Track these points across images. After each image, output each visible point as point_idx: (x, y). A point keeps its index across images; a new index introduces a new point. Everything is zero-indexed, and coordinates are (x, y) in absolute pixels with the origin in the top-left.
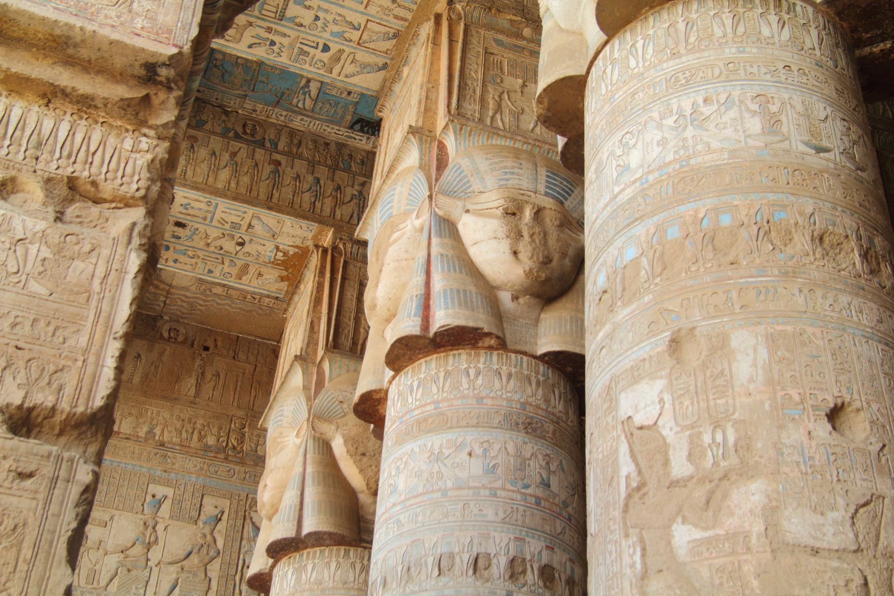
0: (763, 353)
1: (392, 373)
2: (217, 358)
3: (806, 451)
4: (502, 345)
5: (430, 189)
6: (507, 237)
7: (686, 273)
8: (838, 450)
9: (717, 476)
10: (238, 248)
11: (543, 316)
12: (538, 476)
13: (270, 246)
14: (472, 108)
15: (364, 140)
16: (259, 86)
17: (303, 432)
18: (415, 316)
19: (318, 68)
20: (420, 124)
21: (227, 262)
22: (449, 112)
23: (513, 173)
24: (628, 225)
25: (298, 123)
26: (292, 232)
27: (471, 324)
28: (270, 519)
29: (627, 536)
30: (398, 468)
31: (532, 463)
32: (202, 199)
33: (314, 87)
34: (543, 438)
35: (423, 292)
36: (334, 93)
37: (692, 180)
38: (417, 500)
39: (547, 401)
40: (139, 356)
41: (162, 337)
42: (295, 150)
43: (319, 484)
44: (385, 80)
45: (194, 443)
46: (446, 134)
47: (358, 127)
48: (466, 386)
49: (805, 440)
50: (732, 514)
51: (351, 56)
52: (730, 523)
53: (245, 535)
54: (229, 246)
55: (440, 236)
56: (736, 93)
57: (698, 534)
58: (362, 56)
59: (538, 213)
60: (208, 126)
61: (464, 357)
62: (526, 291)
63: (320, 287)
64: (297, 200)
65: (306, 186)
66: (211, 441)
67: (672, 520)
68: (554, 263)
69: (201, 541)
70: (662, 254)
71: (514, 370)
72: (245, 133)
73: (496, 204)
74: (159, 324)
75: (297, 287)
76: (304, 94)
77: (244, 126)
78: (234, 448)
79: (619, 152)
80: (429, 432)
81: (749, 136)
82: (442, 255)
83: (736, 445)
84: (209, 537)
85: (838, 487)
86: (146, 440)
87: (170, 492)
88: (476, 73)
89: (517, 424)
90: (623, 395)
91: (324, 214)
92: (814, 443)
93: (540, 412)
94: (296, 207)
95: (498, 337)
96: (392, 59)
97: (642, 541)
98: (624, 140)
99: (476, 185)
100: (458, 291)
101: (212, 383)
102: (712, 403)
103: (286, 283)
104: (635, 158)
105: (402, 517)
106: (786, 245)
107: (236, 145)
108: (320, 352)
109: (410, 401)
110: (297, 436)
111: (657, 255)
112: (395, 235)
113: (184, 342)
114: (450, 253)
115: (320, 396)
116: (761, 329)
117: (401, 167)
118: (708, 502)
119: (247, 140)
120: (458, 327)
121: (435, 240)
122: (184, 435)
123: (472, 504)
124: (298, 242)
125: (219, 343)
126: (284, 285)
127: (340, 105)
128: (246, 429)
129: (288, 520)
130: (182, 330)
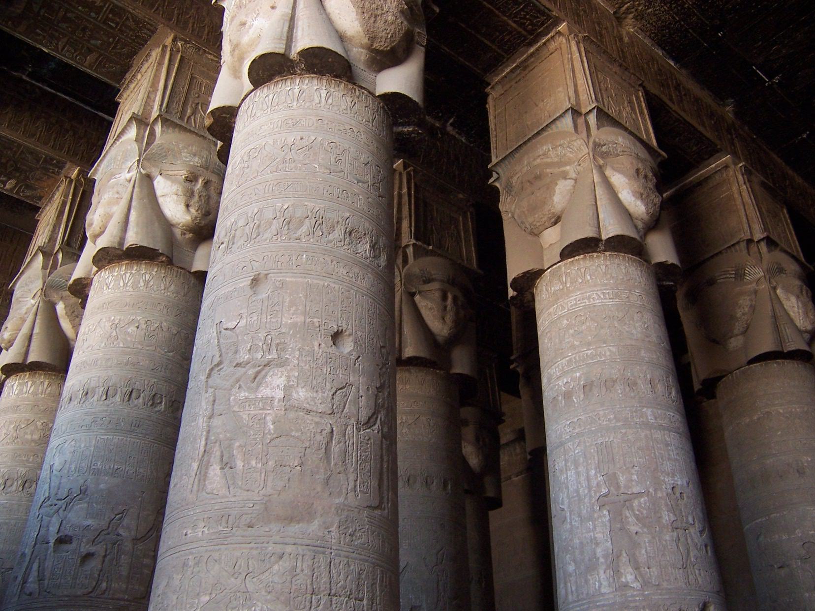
3: (315, 355)
4: (170, 262)
5: (140, 156)
22: (160, 109)
27: (151, 246)
29: (206, 392)
52: (265, 392)
59: (207, 184)
63: (64, 204)
70: (259, 226)
95: (167, 257)
106: (329, 234)
115: (52, 275)
118: (255, 378)
121: (136, 190)
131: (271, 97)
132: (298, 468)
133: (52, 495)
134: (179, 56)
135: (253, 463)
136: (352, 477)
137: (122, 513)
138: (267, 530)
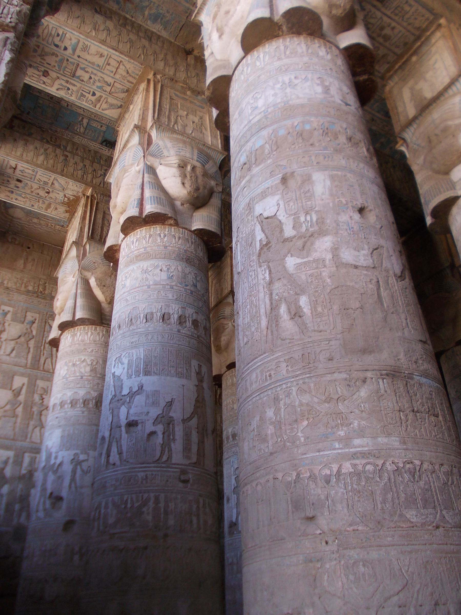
0: (328, 183)
1: (124, 236)
3: (350, 225)
4: (176, 224)
5: (144, 153)
6: (180, 176)
7: (289, 149)
8: (363, 225)
9: (308, 235)
10: (46, 194)
11: (194, 214)
13: (62, 194)
14: (164, 120)
15: (107, 150)
17: (76, 275)
19: (89, 104)
20: (140, 124)
21: (41, 202)
23: (183, 150)
24: (258, 131)
25: (76, 139)
26: (72, 188)
27: (163, 212)
28: (60, 314)
29: (260, 266)
30: (126, 277)
35: (140, 197)
36: (94, 126)
37: (291, 110)
38: (135, 290)
39: (196, 251)
42: (75, 152)
43: (83, 297)
44: (121, 114)
46: (152, 130)
47: (104, 144)
48: (159, 241)
49: (349, 220)
50: (316, 251)
52: (315, 255)
53: (46, 330)
54: (42, 193)
55: (149, 173)
56: (310, 76)
57: (299, 261)
58: (111, 100)
59: (194, 168)
61: (158, 228)
62: (188, 202)
63: (85, 212)
64: (75, 173)
65: (79, 168)
67: (286, 256)
68: (201, 190)
70: (276, 142)
71: (181, 236)
75: (74, 214)
76: (81, 125)
77: (51, 138)
78: (41, 292)
79: (252, 102)
80: (141, 260)
81: (316, 93)
82: (149, 182)
83: (317, 221)
85: (365, 241)
88: (166, 106)
90: (257, 205)
91: (88, 181)
92: (353, 222)
93: (193, 255)
94: (75, 176)
95: (175, 220)
96: (125, 103)
97: (269, 267)
98: (254, 96)
99: (166, 153)
100: (157, 197)
102: (304, 204)
103: (68, 214)
104: (260, 103)
105: (128, 298)
107: (47, 146)
108: (85, 240)
109: (132, 247)
111: (274, 142)
112: (127, 174)
114: (153, 181)
115: (85, 260)
116: (327, 172)
117: (129, 145)
119: (52, 144)
120: (156, 213)
121: (146, 175)
123: (162, 292)
124: (75, 193)
126: (67, 215)
128: (47, 284)
129: (69, 313)
131: (261, 56)
132: (359, 310)
133: (117, 393)
134: (160, 85)
135: (319, 309)
136: (403, 316)
137: (171, 401)
138: (347, 360)
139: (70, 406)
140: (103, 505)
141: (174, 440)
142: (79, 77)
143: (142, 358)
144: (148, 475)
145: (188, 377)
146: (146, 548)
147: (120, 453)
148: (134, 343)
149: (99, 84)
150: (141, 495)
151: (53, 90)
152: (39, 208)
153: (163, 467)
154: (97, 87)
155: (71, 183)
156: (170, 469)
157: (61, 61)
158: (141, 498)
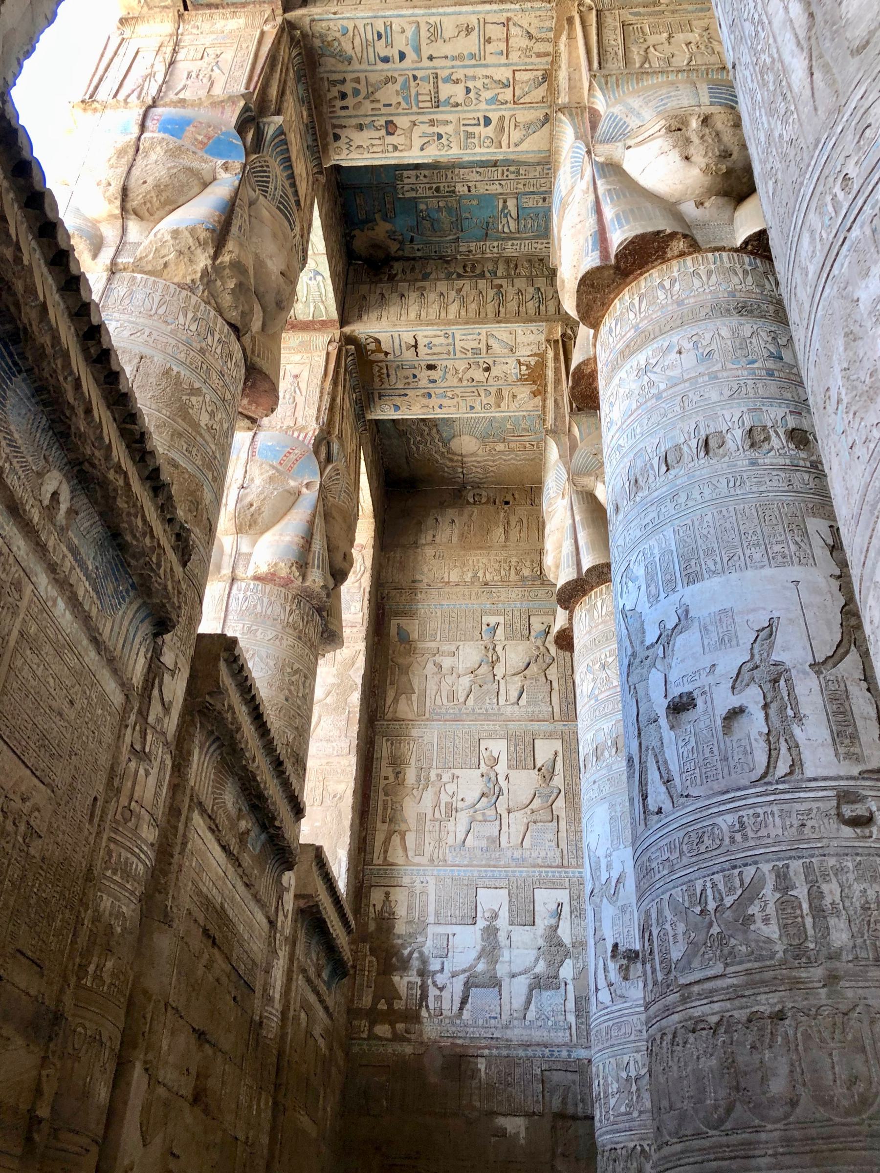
1: (592, 331)
2: (517, 508)
4: (694, 247)
6: (674, 147)
10: (486, 374)
11: (736, 214)
12: (764, 351)
16: (466, 223)
18: (593, 251)
21: (482, 393)
25: (511, 249)
31: (754, 340)
32: (439, 333)
33: (511, 204)
34: (764, 317)
36: (531, 205)
38: (632, 418)
40: (453, 521)
41: (468, 503)
43: (588, 527)
45: (513, 577)
46: (594, 96)
51: (513, 120)
54: (479, 375)
55: (605, 177)
58: (525, 116)
59: (706, 120)
60: (432, 277)
62: (711, 192)
64: (523, 309)
65: (528, 297)
66: (526, 572)
69: (536, 653)
71: (713, 267)
72: (466, 271)
73: (657, 127)
74: (464, 493)
76: (506, 216)
77: (464, 267)
84: (542, 648)
86: (472, 583)
87: (501, 619)
89: (728, 310)
91: (549, 313)
93: (754, 296)
95: (685, 236)
101: (518, 528)
105: (621, 442)
107: (460, 283)
110: (563, 497)
113: (487, 503)
120: (636, 237)
121: (599, 183)
122: (503, 573)
123: (691, 394)
125: (517, 496)
126: (538, 400)
127: (541, 216)
130: (484, 494)
133: (638, 648)
137: (770, 625)
139: (614, 750)
140: (654, 916)
141: (798, 717)
142: (447, 102)
143: (674, 548)
144: (745, 819)
145: (806, 559)
146: (780, 1016)
147: (667, 782)
148: (651, 525)
149: (487, 95)
150: (736, 872)
151: (414, 156)
152: (486, 407)
153: (784, 792)
154: (488, 102)
155: (519, 332)
156: (803, 795)
157: (406, 86)
158: (737, 883)
